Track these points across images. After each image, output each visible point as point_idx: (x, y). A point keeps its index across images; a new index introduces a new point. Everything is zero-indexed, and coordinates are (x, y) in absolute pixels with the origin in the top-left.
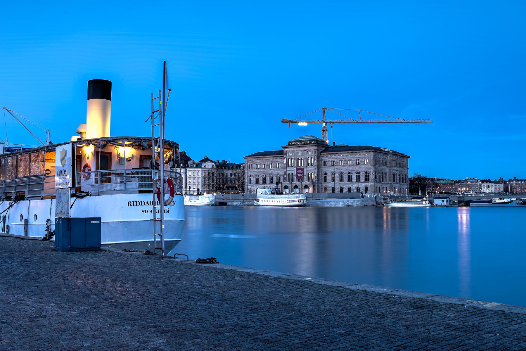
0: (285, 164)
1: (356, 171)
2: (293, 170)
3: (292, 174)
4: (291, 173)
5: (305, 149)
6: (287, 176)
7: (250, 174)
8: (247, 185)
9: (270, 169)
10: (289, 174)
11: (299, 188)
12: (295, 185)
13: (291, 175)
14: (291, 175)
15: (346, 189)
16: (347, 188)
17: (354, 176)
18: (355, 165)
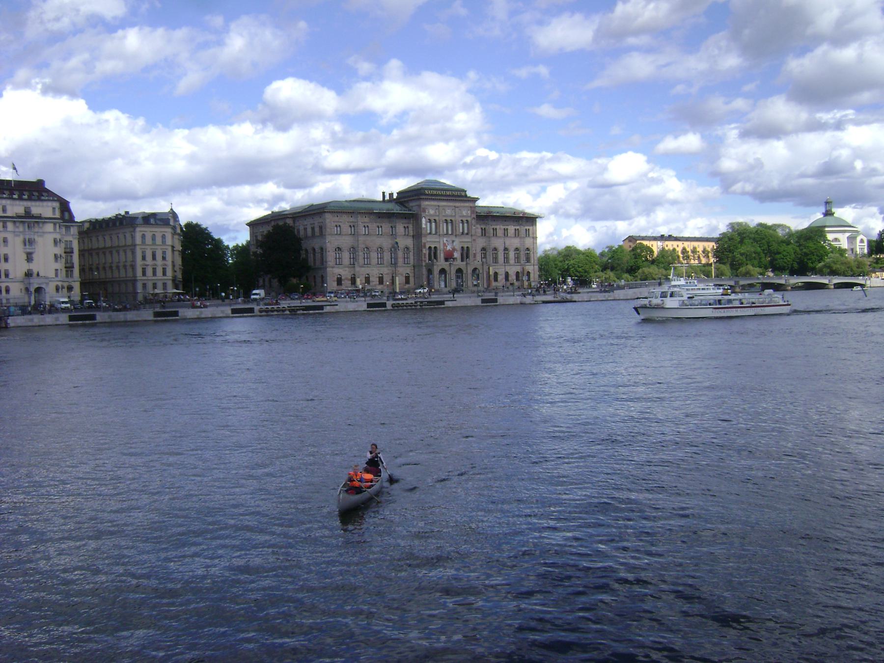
0: (424, 228)
1: (515, 247)
2: (437, 240)
3: (435, 248)
4: (433, 246)
5: (457, 204)
6: (428, 252)
7: (336, 244)
8: (333, 267)
9: (378, 237)
10: (430, 248)
11: (464, 272)
12: (458, 267)
13: (433, 249)
14: (433, 249)
15: (501, 275)
16: (504, 273)
17: (512, 255)
18: (514, 237)
